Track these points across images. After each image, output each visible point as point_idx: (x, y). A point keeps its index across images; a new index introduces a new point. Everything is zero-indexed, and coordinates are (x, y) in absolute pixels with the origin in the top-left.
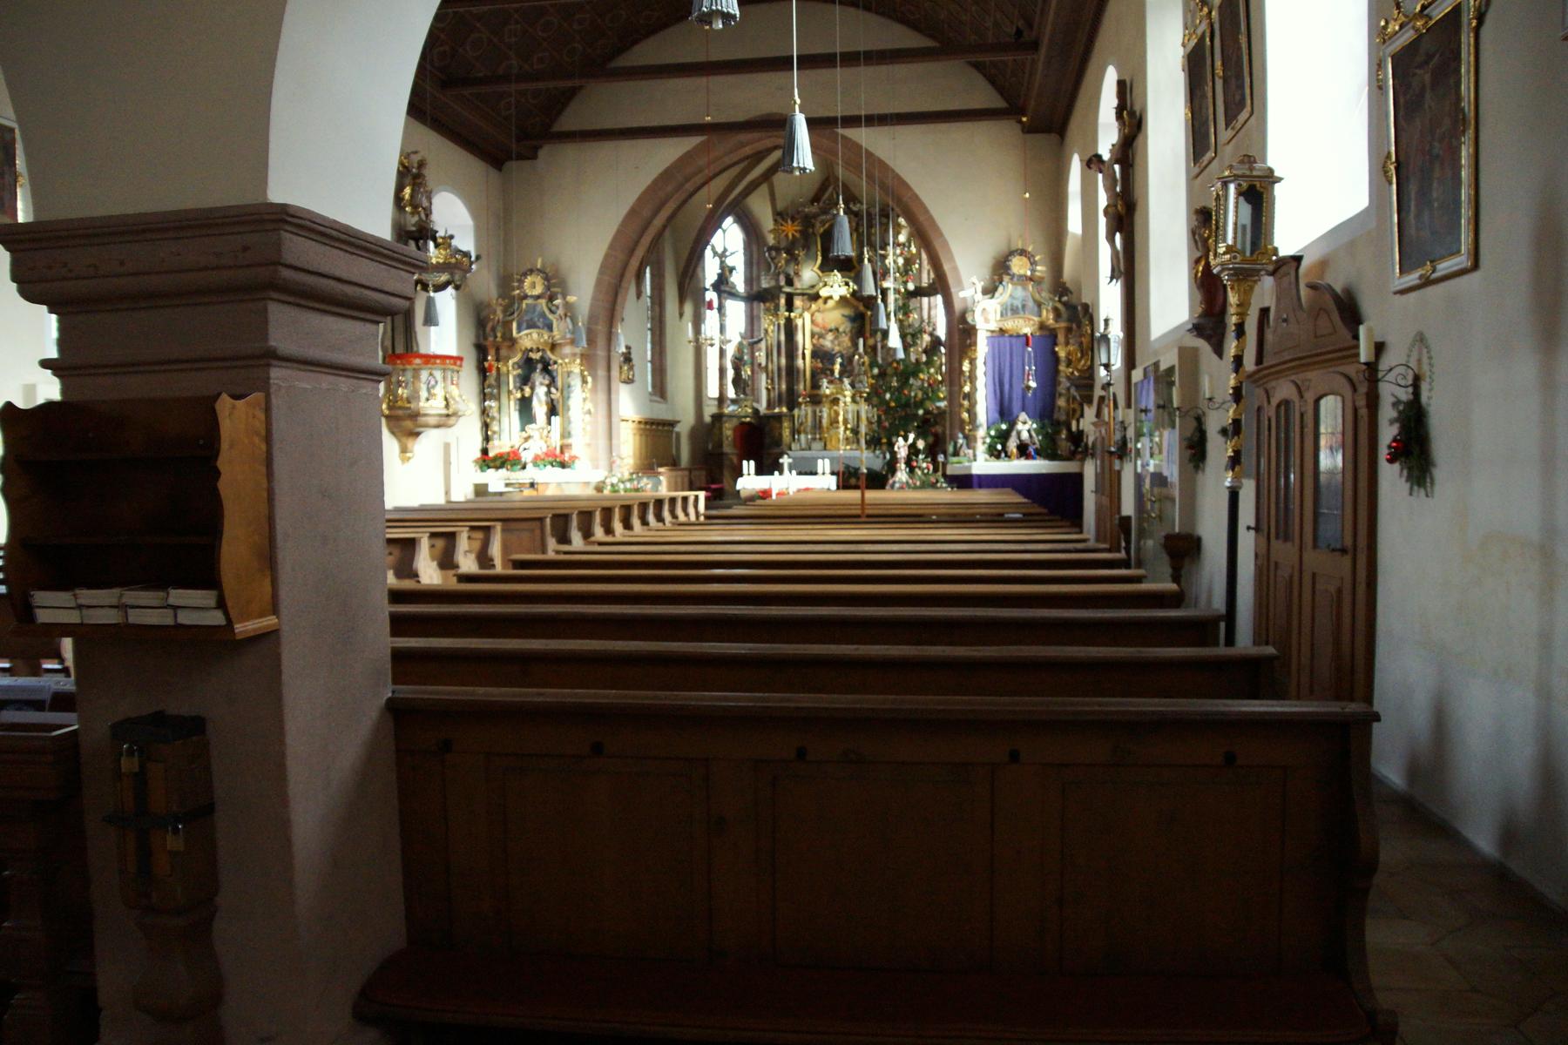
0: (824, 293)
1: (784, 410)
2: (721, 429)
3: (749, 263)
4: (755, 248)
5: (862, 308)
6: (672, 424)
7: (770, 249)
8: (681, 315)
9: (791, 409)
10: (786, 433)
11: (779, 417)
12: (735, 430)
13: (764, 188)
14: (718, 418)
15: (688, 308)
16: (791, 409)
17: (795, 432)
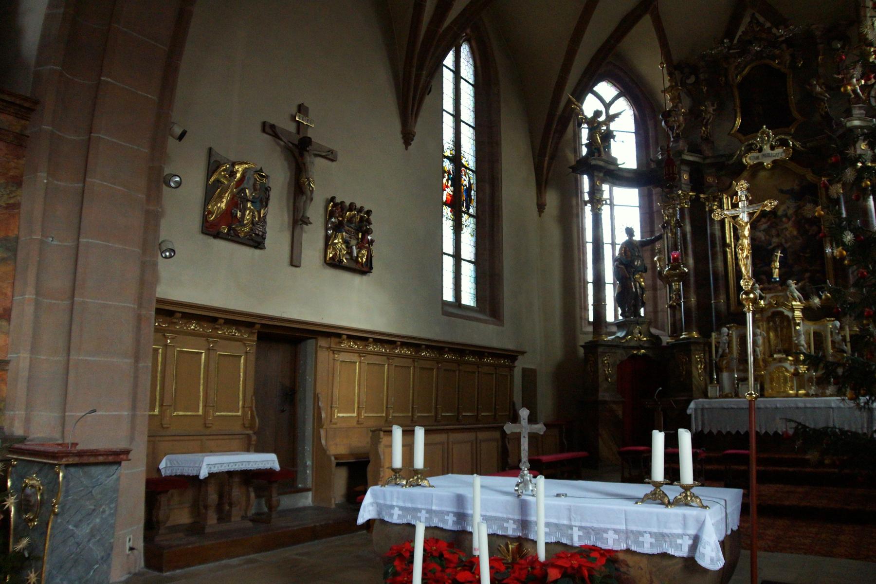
0: (749, 160)
1: (695, 334)
2: (596, 364)
3: (643, 145)
4: (650, 124)
5: (810, 177)
6: (512, 356)
7: (667, 115)
8: (541, 207)
9: (706, 333)
10: (699, 369)
11: (687, 346)
12: (621, 367)
13: (646, 21)
14: (592, 347)
15: (552, 199)
16: (706, 333)
17: (714, 368)
